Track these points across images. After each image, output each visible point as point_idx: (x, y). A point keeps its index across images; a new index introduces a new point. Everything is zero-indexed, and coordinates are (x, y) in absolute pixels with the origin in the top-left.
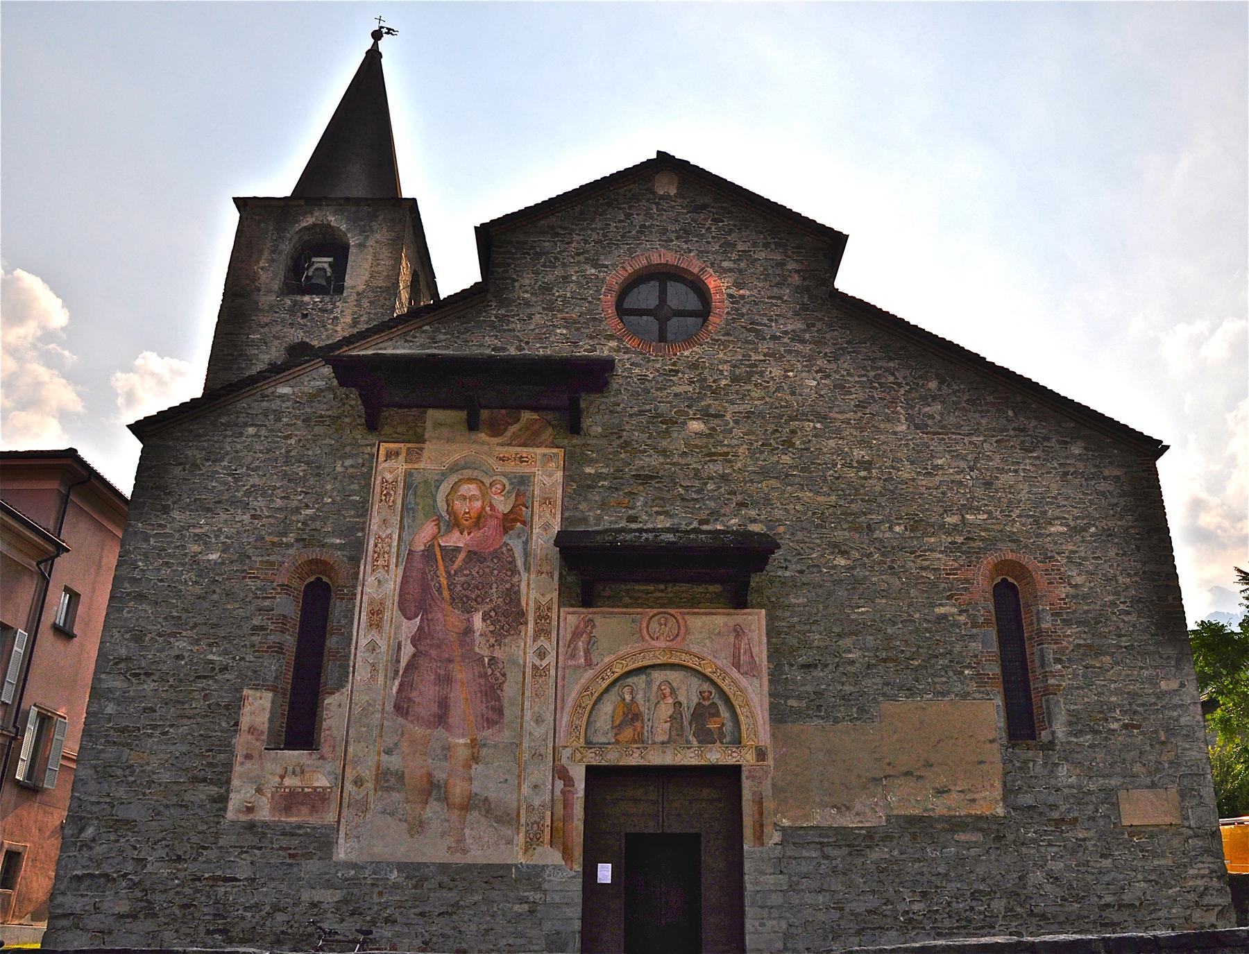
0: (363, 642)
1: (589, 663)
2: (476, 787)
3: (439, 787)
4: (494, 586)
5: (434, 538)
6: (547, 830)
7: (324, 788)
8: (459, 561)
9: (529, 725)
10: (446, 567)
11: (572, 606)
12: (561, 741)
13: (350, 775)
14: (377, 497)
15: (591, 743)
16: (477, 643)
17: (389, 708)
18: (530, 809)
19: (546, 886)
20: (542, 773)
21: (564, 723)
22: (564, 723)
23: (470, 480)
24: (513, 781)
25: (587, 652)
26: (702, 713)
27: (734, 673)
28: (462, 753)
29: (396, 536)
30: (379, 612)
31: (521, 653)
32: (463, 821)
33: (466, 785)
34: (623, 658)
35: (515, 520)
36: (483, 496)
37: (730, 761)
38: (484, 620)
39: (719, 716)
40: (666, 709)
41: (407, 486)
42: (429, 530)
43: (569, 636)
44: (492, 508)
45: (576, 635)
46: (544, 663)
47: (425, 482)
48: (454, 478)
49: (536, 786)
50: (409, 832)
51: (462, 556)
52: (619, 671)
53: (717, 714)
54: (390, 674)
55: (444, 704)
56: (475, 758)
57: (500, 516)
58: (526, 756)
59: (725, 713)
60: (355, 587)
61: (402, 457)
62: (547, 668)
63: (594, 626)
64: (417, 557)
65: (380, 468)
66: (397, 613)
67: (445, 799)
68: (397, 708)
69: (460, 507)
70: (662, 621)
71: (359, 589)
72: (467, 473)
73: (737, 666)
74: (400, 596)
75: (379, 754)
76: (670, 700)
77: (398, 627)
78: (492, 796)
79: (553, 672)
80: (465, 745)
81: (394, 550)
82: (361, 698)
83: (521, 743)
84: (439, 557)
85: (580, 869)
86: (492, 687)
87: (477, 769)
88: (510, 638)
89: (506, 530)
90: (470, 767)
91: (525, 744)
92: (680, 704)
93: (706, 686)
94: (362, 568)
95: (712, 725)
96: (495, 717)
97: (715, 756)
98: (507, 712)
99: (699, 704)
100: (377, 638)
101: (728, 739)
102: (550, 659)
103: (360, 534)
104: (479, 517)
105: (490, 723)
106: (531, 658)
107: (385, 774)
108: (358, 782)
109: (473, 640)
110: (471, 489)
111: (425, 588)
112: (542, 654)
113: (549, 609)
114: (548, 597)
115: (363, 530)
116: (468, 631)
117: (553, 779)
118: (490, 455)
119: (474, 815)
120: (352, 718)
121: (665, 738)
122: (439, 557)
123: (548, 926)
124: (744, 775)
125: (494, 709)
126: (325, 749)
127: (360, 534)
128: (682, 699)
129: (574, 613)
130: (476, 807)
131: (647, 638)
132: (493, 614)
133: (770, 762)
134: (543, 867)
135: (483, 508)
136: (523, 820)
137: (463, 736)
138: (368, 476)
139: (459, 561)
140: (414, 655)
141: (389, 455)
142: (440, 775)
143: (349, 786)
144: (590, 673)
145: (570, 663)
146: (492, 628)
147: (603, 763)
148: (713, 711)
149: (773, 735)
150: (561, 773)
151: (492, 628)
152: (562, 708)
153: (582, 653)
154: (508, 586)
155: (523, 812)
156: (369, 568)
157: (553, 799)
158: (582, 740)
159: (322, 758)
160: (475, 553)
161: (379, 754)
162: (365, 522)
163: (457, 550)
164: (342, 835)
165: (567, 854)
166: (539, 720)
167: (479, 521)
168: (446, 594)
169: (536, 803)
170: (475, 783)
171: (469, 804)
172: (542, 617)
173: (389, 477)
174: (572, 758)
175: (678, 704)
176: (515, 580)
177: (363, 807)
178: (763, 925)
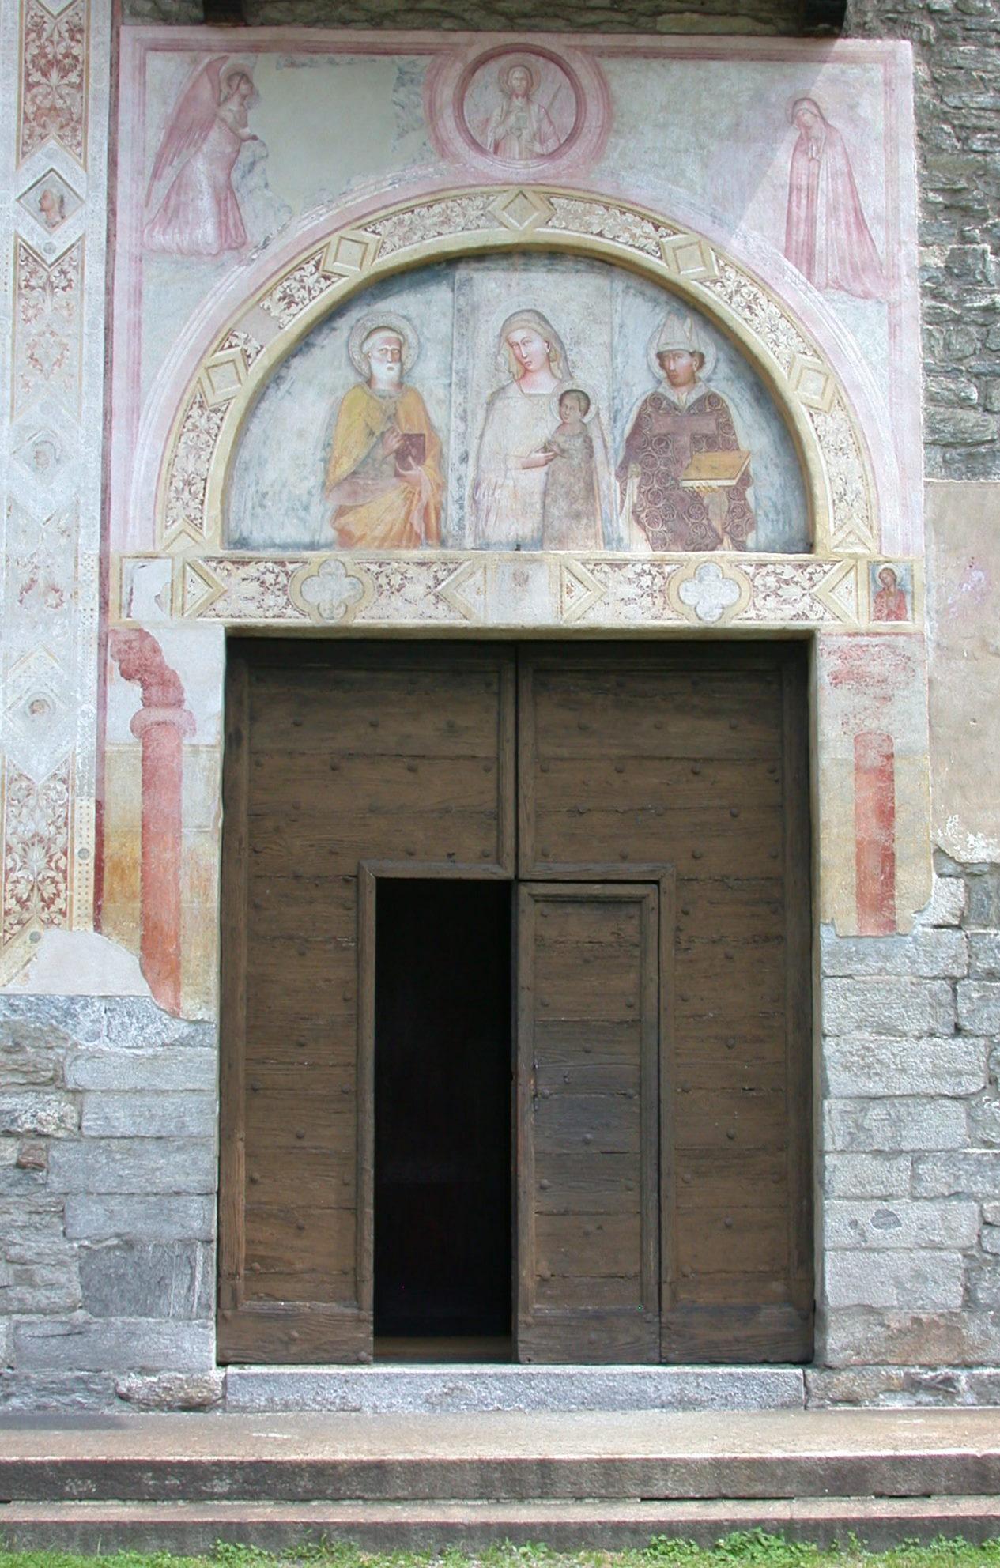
1: (234, 239)
6: (83, 871)
12: (133, 531)
15: (242, 543)
19: (78, 1075)
21: (140, 470)
22: (140, 470)
25: (227, 197)
26: (662, 442)
27: (791, 281)
34: (363, 221)
37: (769, 614)
39: (731, 446)
40: (529, 419)
43: (155, 137)
45: (182, 132)
46: (63, 238)
49: (35, 707)
52: (351, 271)
53: (721, 439)
59: (752, 434)
62: (69, 263)
63: (250, 97)
70: (517, 78)
73: (806, 257)
76: (545, 385)
79: (94, 273)
85: (209, 1012)
92: (585, 400)
93: (684, 334)
95: (706, 480)
97: (721, 593)
99: (655, 401)
101: (764, 531)
102: (85, 222)
112: (51, 206)
113: (76, 31)
117: (103, 679)
121: (526, 528)
123: (91, 1219)
124: (826, 665)
128: (590, 376)
129: (174, 47)
131: (459, 144)
133: (920, 621)
134: (69, 1010)
144: (237, 279)
145: (159, 239)
147: (292, 619)
148: (708, 426)
149: (936, 524)
150: (140, 664)
152: (135, 410)
153: (206, 203)
157: (101, 755)
158: (211, 533)
165: (157, 954)
169: (40, 768)
174: (172, 599)
175: (574, 399)
178: (887, 1219)
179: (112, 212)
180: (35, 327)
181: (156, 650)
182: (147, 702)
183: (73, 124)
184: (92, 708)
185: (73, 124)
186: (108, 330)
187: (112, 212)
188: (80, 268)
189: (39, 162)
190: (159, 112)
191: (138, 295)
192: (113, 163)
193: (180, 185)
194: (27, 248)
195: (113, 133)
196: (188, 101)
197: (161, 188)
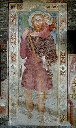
0: (10, 66)
2: (46, 106)
3: (35, 106)
4: (48, 48)
5: (29, 34)
6: (66, 117)
7: (4, 107)
8: (37, 41)
9: (60, 88)
10: (33, 43)
11: (71, 54)
13: (11, 103)
14: (10, 21)
16: (44, 65)
17: (20, 84)
18: (61, 111)
20: (64, 102)
22: (70, 88)
23: (38, 15)
24: (56, 104)
28: (42, 97)
29: (17, 33)
30: (14, 57)
31: (57, 68)
32: (43, 114)
33: (43, 105)
35: (53, 27)
36: (43, 20)
38: (45, 58)
41: (19, 17)
42: (27, 31)
43: (71, 63)
44: (46, 24)
47: (24, 15)
48: (33, 14)
50: (28, 117)
51: (37, 39)
54: (19, 75)
55: (35, 83)
56: (45, 98)
57: (48, 26)
58: (59, 97)
60: (6, 49)
61: (16, 7)
64: (24, 40)
65: (10, 11)
66: (20, 57)
67: (38, 109)
68: (22, 84)
69: (36, 24)
71: (8, 50)
72: (37, 12)
74: (20, 52)
75: (18, 97)
77: (20, 61)
78: (51, 108)
79: (66, 73)
80: (42, 94)
81: (17, 38)
82: (11, 82)
83: (58, 93)
84: (31, 40)
86: (49, 78)
87: (46, 101)
88: (53, 63)
89: (50, 31)
90: (44, 100)
91: (59, 94)
94: (8, 43)
96: (50, 86)
98: (53, 85)
100: (14, 64)
102: (66, 70)
103: (6, 33)
104: (42, 27)
105: (49, 88)
106: (60, 69)
107: (20, 102)
108: (13, 105)
109: (43, 64)
110: (39, 18)
111: (27, 49)
112: (63, 68)
113: (64, 55)
114: (64, 51)
115: (7, 31)
116: (41, 62)
117: (67, 103)
118: (44, 6)
119: (46, 113)
120: (10, 87)
122: (31, 40)
125: (50, 84)
126: (3, 96)
127: (6, 33)
129: (72, 56)
130: (46, 111)
132: (48, 57)
135: (43, 24)
136: (59, 114)
137: (42, 92)
138: (6, 14)
139: (37, 41)
140: (26, 69)
141: (12, 7)
142: (36, 102)
143: (10, 106)
146: (48, 61)
150: (70, 102)
151: (48, 61)
152: (69, 84)
154: (52, 48)
155: (59, 112)
156: (10, 43)
159: (2, 98)
160: (42, 38)
161: (18, 97)
162: (7, 29)
163: (36, 37)
164: (10, 119)
165: (72, 123)
166: (63, 87)
167: (42, 28)
168: (34, 51)
169: (63, 110)
170: (46, 104)
171: (44, 110)
172: (62, 57)
173: (13, 14)
176: (54, 46)
177: (15, 111)
179: (68, 69)
180: (62, 77)
181: (71, 101)
182: (71, 105)
183: (64, 62)
184: (67, 105)
185: (64, 62)
186: (67, 78)
187: (68, 69)
188: (65, 73)
189: (62, 65)
190: (71, 61)
191: (70, 75)
192: (67, 65)
193: (73, 67)
194: (61, 72)
195: (67, 63)
196: (73, 60)
197: (71, 67)
